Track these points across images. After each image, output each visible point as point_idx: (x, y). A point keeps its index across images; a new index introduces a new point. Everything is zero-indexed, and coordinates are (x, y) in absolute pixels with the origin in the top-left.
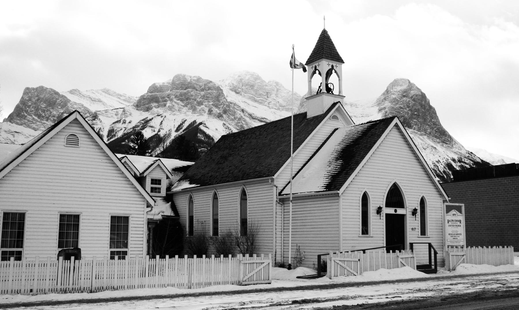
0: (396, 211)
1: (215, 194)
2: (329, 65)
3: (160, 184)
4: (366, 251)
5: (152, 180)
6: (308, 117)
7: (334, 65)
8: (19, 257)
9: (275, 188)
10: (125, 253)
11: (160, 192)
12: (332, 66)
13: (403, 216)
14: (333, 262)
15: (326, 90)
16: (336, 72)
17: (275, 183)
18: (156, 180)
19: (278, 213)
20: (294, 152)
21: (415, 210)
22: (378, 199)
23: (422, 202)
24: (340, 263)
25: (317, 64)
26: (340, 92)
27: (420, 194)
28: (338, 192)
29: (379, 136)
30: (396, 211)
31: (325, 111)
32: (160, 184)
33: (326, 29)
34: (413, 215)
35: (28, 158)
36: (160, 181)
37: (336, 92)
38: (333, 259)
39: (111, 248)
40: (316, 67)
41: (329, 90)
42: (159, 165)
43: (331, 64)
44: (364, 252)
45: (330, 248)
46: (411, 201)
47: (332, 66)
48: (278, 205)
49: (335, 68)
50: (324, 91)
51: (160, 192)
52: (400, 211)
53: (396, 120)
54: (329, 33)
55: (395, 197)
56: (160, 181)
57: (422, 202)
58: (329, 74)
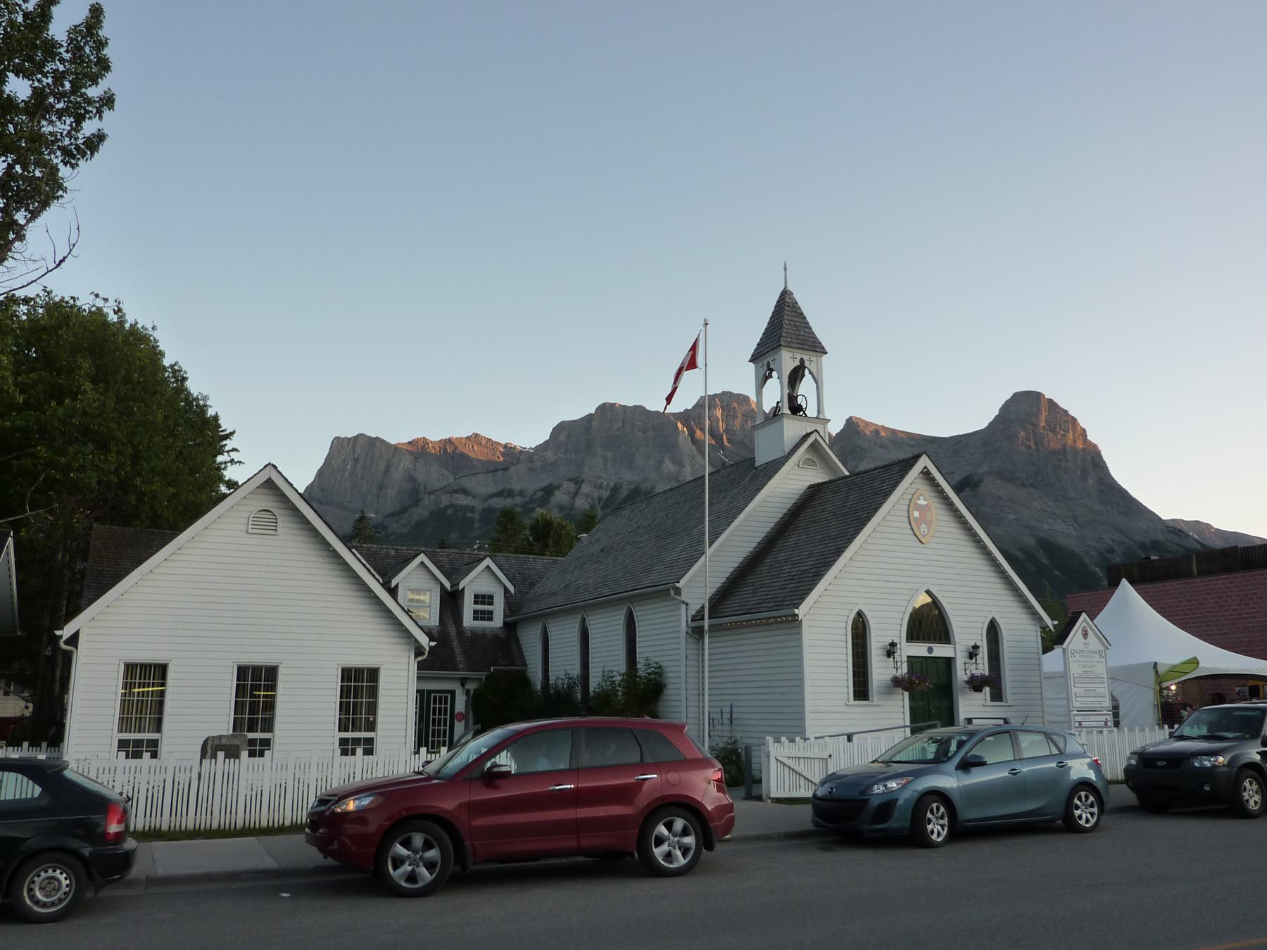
0: (930, 650)
1: (583, 621)
2: (794, 358)
3: (491, 603)
4: (855, 737)
5: (476, 596)
6: (757, 464)
7: (806, 358)
8: (154, 748)
9: (684, 607)
10: (266, 743)
11: (491, 619)
12: (802, 361)
13: (949, 662)
14: (772, 760)
15: (790, 408)
16: (810, 372)
17: (684, 597)
18: (483, 596)
19: (690, 657)
20: (714, 537)
21: (976, 647)
22: (888, 627)
23: (993, 630)
24: (788, 762)
25: (770, 359)
26: (819, 412)
27: (850, 607)
28: (796, 611)
29: (887, 495)
30: (930, 650)
31: (787, 450)
32: (491, 603)
33: (790, 288)
34: (971, 658)
35: (172, 557)
36: (491, 597)
37: (811, 411)
38: (772, 755)
39: (120, 731)
40: (769, 364)
41: (796, 409)
42: (488, 567)
43: (799, 357)
44: (850, 738)
45: (766, 729)
46: (967, 631)
47: (802, 361)
48: (690, 640)
49: (807, 364)
50: (786, 411)
51: (491, 619)
52: (941, 651)
53: (924, 462)
54: (797, 296)
55: (929, 623)
56: (491, 597)
57: (993, 630)
58: (795, 377)
